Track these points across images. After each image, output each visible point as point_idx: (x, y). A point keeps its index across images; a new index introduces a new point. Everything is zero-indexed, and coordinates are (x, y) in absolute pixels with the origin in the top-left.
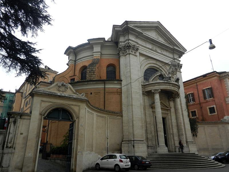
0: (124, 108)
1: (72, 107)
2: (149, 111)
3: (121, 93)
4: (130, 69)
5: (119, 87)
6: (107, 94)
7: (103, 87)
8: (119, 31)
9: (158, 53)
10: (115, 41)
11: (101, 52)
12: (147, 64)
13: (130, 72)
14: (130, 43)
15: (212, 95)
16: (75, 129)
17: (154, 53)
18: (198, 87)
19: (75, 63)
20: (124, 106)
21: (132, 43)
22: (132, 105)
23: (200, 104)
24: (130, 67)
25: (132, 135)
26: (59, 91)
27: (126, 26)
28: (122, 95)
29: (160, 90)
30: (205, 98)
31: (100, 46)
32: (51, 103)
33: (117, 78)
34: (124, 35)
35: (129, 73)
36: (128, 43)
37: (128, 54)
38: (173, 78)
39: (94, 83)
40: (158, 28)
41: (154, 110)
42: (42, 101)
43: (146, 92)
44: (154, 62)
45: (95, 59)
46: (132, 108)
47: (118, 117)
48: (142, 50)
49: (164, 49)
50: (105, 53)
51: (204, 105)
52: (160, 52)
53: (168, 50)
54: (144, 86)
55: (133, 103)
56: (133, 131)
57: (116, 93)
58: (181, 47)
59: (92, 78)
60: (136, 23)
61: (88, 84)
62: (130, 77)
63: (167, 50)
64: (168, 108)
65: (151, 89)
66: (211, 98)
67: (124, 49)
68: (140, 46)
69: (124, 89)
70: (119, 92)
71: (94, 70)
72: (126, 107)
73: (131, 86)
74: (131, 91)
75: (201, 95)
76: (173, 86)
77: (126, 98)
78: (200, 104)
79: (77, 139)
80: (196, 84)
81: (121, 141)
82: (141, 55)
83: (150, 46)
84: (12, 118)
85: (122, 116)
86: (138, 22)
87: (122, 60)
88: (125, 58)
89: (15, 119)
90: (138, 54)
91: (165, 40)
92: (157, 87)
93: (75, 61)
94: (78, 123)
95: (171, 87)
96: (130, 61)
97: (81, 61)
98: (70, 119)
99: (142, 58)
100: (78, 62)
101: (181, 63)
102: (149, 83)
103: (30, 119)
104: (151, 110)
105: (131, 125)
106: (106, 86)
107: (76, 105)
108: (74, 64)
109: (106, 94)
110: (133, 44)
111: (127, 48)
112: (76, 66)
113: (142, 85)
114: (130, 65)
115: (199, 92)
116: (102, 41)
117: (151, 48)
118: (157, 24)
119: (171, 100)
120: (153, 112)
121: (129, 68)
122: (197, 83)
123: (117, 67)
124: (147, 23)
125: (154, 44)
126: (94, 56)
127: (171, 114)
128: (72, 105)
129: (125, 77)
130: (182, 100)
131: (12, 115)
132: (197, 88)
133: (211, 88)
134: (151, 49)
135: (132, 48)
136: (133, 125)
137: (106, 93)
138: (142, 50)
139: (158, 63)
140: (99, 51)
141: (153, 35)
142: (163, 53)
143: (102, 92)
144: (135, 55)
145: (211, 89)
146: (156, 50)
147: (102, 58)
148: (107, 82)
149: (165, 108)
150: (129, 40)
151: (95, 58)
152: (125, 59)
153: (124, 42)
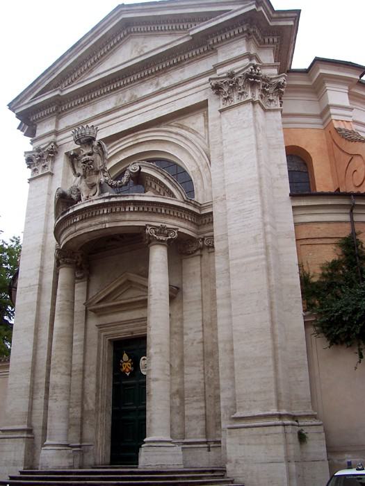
17: (119, 117)
63: (179, 64)
91: (172, 32)
95: (77, 227)
124: (73, 51)
125: (118, 88)
139: (129, 141)
141: (125, 56)
142: (165, 85)
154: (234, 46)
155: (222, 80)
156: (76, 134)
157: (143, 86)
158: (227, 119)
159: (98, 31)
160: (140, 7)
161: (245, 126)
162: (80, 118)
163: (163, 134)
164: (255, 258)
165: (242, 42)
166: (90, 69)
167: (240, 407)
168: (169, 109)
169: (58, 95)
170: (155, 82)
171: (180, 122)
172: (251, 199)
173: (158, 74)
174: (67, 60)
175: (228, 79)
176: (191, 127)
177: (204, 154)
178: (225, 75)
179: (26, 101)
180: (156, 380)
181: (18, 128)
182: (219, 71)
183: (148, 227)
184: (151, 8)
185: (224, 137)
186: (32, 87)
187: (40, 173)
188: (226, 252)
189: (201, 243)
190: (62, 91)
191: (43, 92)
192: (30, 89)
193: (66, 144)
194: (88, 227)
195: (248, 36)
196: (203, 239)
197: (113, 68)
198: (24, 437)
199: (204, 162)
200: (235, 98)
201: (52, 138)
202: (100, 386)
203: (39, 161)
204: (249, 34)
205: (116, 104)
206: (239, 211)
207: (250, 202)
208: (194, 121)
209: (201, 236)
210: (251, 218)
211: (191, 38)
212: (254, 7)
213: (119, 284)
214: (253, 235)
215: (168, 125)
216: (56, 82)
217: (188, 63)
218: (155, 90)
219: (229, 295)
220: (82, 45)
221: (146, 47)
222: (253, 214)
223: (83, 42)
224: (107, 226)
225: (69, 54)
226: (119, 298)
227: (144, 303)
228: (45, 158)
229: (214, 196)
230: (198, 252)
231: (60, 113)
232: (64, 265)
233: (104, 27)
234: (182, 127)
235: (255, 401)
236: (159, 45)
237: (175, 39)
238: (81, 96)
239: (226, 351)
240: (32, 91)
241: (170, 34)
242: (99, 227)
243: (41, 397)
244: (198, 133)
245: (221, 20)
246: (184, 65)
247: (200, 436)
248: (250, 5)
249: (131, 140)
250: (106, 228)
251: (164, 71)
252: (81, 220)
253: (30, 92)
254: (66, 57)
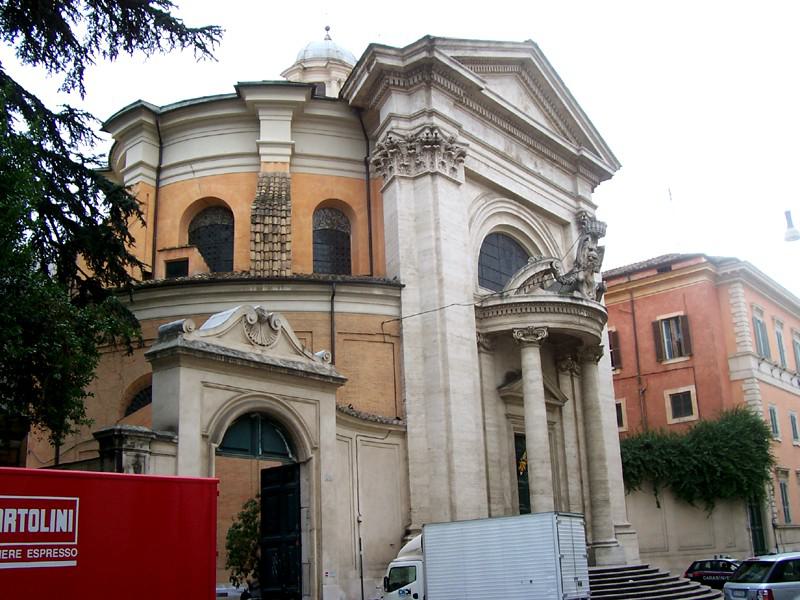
0: (413, 403)
1: (295, 406)
2: (497, 412)
3: (399, 337)
4: (438, 239)
5: (388, 310)
6: (341, 340)
7: (326, 307)
8: (392, 70)
9: (528, 171)
10: (359, 103)
11: (293, 146)
12: (492, 217)
13: (438, 253)
14: (436, 128)
15: (684, 347)
16: (310, 493)
18: (636, 308)
19: (158, 181)
20: (413, 395)
21: (448, 131)
22: (446, 391)
23: (639, 378)
24: (437, 228)
25: (447, 507)
26: (251, 342)
27: (424, 54)
28: (405, 349)
29: (546, 334)
30: (661, 357)
31: (288, 115)
32: (232, 394)
33: (360, 266)
34: (408, 90)
35: (435, 255)
36: (432, 130)
37: (427, 174)
38: (590, 285)
39: (287, 288)
40: (528, 68)
41: (514, 410)
42: (206, 384)
43: (487, 335)
44: (511, 207)
45: (269, 178)
46: (448, 404)
47: (389, 440)
48: (470, 163)
49: (544, 156)
50: (305, 152)
51: (653, 383)
52: (531, 166)
53: (558, 163)
54: (482, 312)
55: (452, 385)
56: (451, 492)
57: (377, 338)
58: (603, 152)
59: (277, 265)
61: (259, 293)
62: (439, 273)
64: (555, 398)
65: (511, 327)
66: (681, 355)
67: (411, 148)
68: (473, 145)
69: (410, 327)
70: (393, 335)
71: (284, 230)
72: (422, 397)
73: (442, 315)
74: (444, 334)
75: (647, 343)
77: (421, 360)
78: (639, 378)
79: (319, 531)
80: (626, 298)
81: (401, 532)
82: (473, 177)
83: (497, 141)
84: (127, 450)
85: (404, 435)
86: (469, 44)
87: (402, 199)
88: (415, 189)
89: (138, 456)
90: (461, 176)
91: (549, 118)
92: (536, 321)
93: (159, 170)
94: (318, 468)
96: (436, 204)
97: (194, 172)
98: (288, 455)
99: (473, 192)
100: (171, 178)
101: (600, 215)
102: (505, 302)
103: (175, 456)
104: (502, 409)
105: (443, 468)
106: (338, 307)
107: (306, 401)
108: (154, 184)
109: (338, 339)
110: (448, 135)
111: (425, 150)
112: (162, 191)
113: (476, 307)
114: (437, 224)
115: (640, 332)
116: (304, 99)
117: (501, 148)
119: (564, 366)
120: (508, 416)
121: (433, 233)
122: (636, 295)
123: (360, 217)
126: (263, 159)
127: (562, 424)
128: (295, 399)
129: (414, 271)
130: (604, 370)
131: (129, 443)
132: (633, 314)
133: (685, 318)
134: (504, 157)
135: (443, 150)
136: (450, 471)
137: (336, 334)
138: (477, 162)
139: (526, 215)
140: (288, 139)
141: (507, 93)
143: (322, 329)
144: (454, 182)
145: (682, 323)
146: (518, 157)
147: (295, 169)
148: (343, 289)
149: (554, 404)
150: (432, 113)
151: (269, 170)
152: (412, 192)
153: (410, 119)
169: (482, 89)
201: (455, 131)
237: (546, 125)
238: (490, 111)
249: (515, 208)
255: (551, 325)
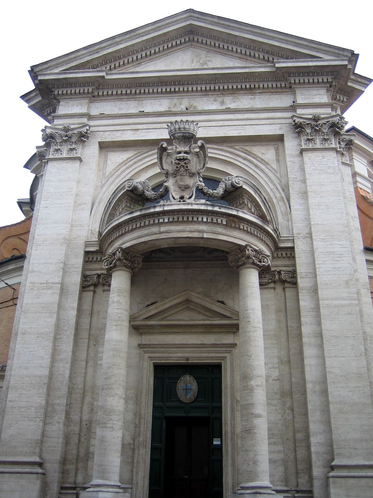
60: (71, 60)
63: (251, 90)
76: (178, 222)
91: (243, 56)
110: (61, 127)
118: (186, 19)
124: (127, 36)
125: (175, 92)
142: (233, 106)
154: (315, 92)
155: (305, 121)
156: (172, 128)
157: (205, 99)
158: (309, 159)
159: (159, 27)
160: (216, 20)
161: (330, 171)
162: (120, 109)
163: (228, 155)
164: (349, 302)
165: (323, 91)
166: (138, 62)
167: (339, 454)
168: (238, 131)
169: (103, 77)
170: (220, 99)
171: (247, 148)
172: (340, 243)
173: (224, 92)
174: (118, 43)
175: (313, 123)
176: (261, 156)
177: (279, 188)
178: (310, 117)
179: (56, 71)
180: (259, 416)
181: (23, 97)
182: (299, 111)
183: (248, 248)
184: (228, 26)
185: (307, 176)
186: (66, 59)
187: (65, 155)
188: (315, 290)
189: (277, 276)
190: (107, 74)
191: (77, 67)
192: (66, 59)
193: (102, 133)
194: (180, 231)
195: (330, 86)
196: (279, 272)
197: (178, 70)
198: (37, 473)
199: (278, 195)
200: (318, 141)
201: (85, 120)
202: (143, 416)
203: (66, 141)
204: (331, 86)
205: (170, 108)
206: (328, 252)
207: (340, 246)
208: (265, 152)
209: (278, 269)
210: (341, 262)
211: (275, 70)
212: (346, 63)
213: (176, 301)
214: (345, 279)
215: (231, 147)
216: (96, 63)
217: (260, 93)
218: (219, 108)
219: (320, 335)
220: (139, 34)
221: (210, 61)
222: (344, 258)
223: (140, 31)
224: (205, 236)
225: (121, 38)
226: (169, 318)
227: (234, 328)
228: (74, 139)
229: (295, 231)
230: (272, 285)
231: (94, 96)
232: (124, 268)
233: (168, 25)
234: (249, 153)
235: (355, 449)
236: (227, 66)
238: (127, 87)
239: (315, 392)
240: (66, 62)
241: (240, 58)
242: (196, 235)
243: (59, 423)
244: (268, 164)
245: (310, 64)
246: (255, 93)
247: (279, 483)
248: (343, 60)
250: (203, 238)
251: (233, 92)
252: (169, 223)
253: (64, 62)
254: (117, 40)
255: (124, 246)
